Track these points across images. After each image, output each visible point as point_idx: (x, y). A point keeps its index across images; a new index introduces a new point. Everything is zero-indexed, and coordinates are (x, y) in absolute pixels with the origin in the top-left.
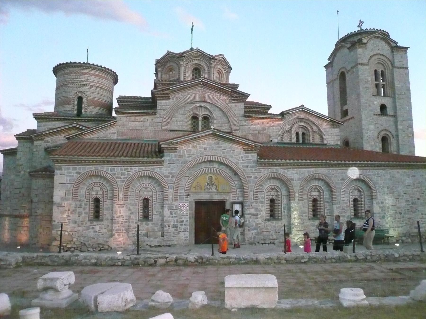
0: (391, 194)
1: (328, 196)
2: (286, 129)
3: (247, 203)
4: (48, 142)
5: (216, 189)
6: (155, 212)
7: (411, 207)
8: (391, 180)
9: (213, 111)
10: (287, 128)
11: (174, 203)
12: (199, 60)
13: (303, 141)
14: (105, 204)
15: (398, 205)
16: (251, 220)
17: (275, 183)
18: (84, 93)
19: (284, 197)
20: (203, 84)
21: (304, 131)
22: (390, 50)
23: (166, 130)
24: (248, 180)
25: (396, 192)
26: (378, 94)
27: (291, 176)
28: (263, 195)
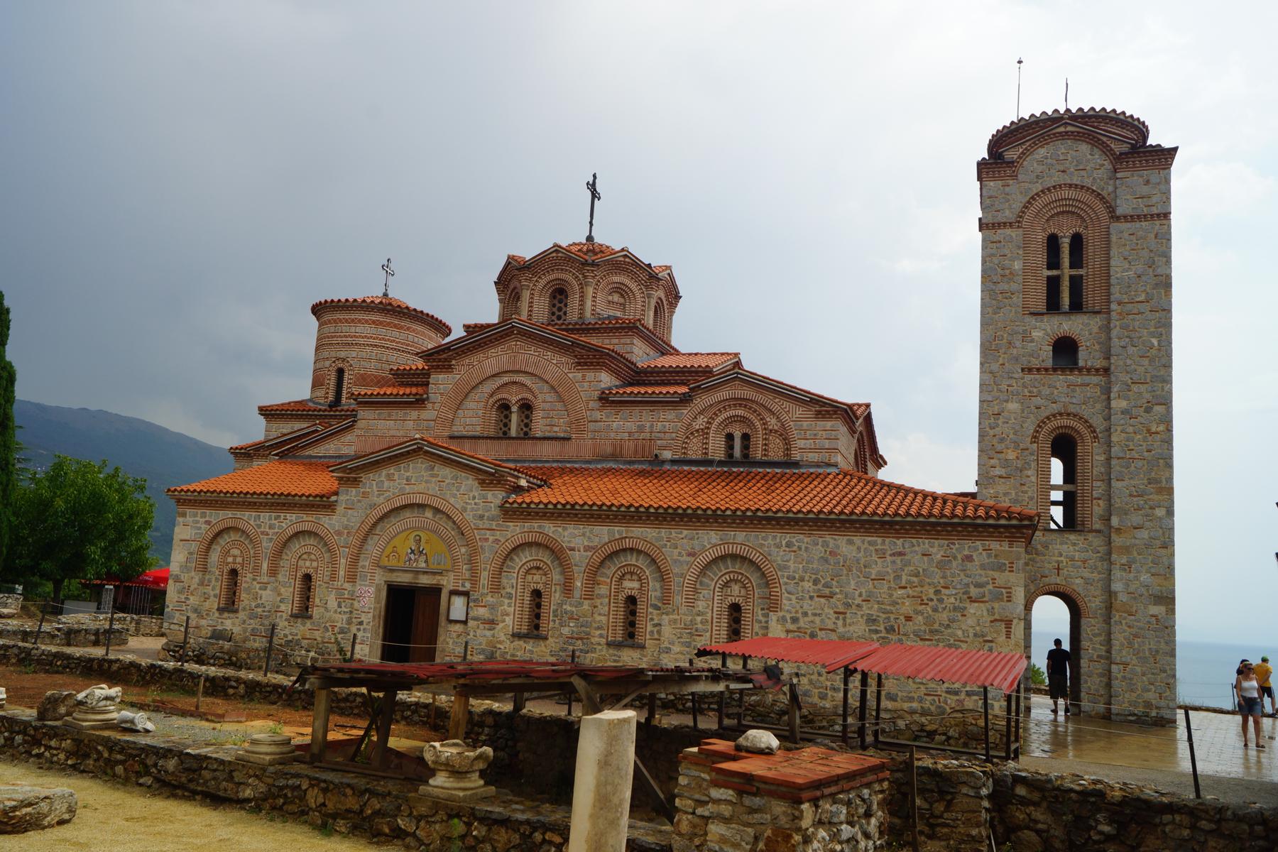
0: (823, 600)
1: (658, 594)
2: (697, 427)
3: (473, 595)
5: (426, 562)
6: (317, 601)
7: (883, 638)
8: (826, 561)
9: (537, 392)
10: (700, 422)
11: (347, 586)
12: (562, 270)
13: (746, 456)
14: (245, 580)
15: (841, 630)
16: (479, 632)
17: (540, 555)
18: (348, 362)
19: (558, 587)
21: (748, 431)
22: (1108, 165)
24: (481, 546)
25: (838, 596)
26: (1053, 305)
27: (569, 542)
28: (514, 581)
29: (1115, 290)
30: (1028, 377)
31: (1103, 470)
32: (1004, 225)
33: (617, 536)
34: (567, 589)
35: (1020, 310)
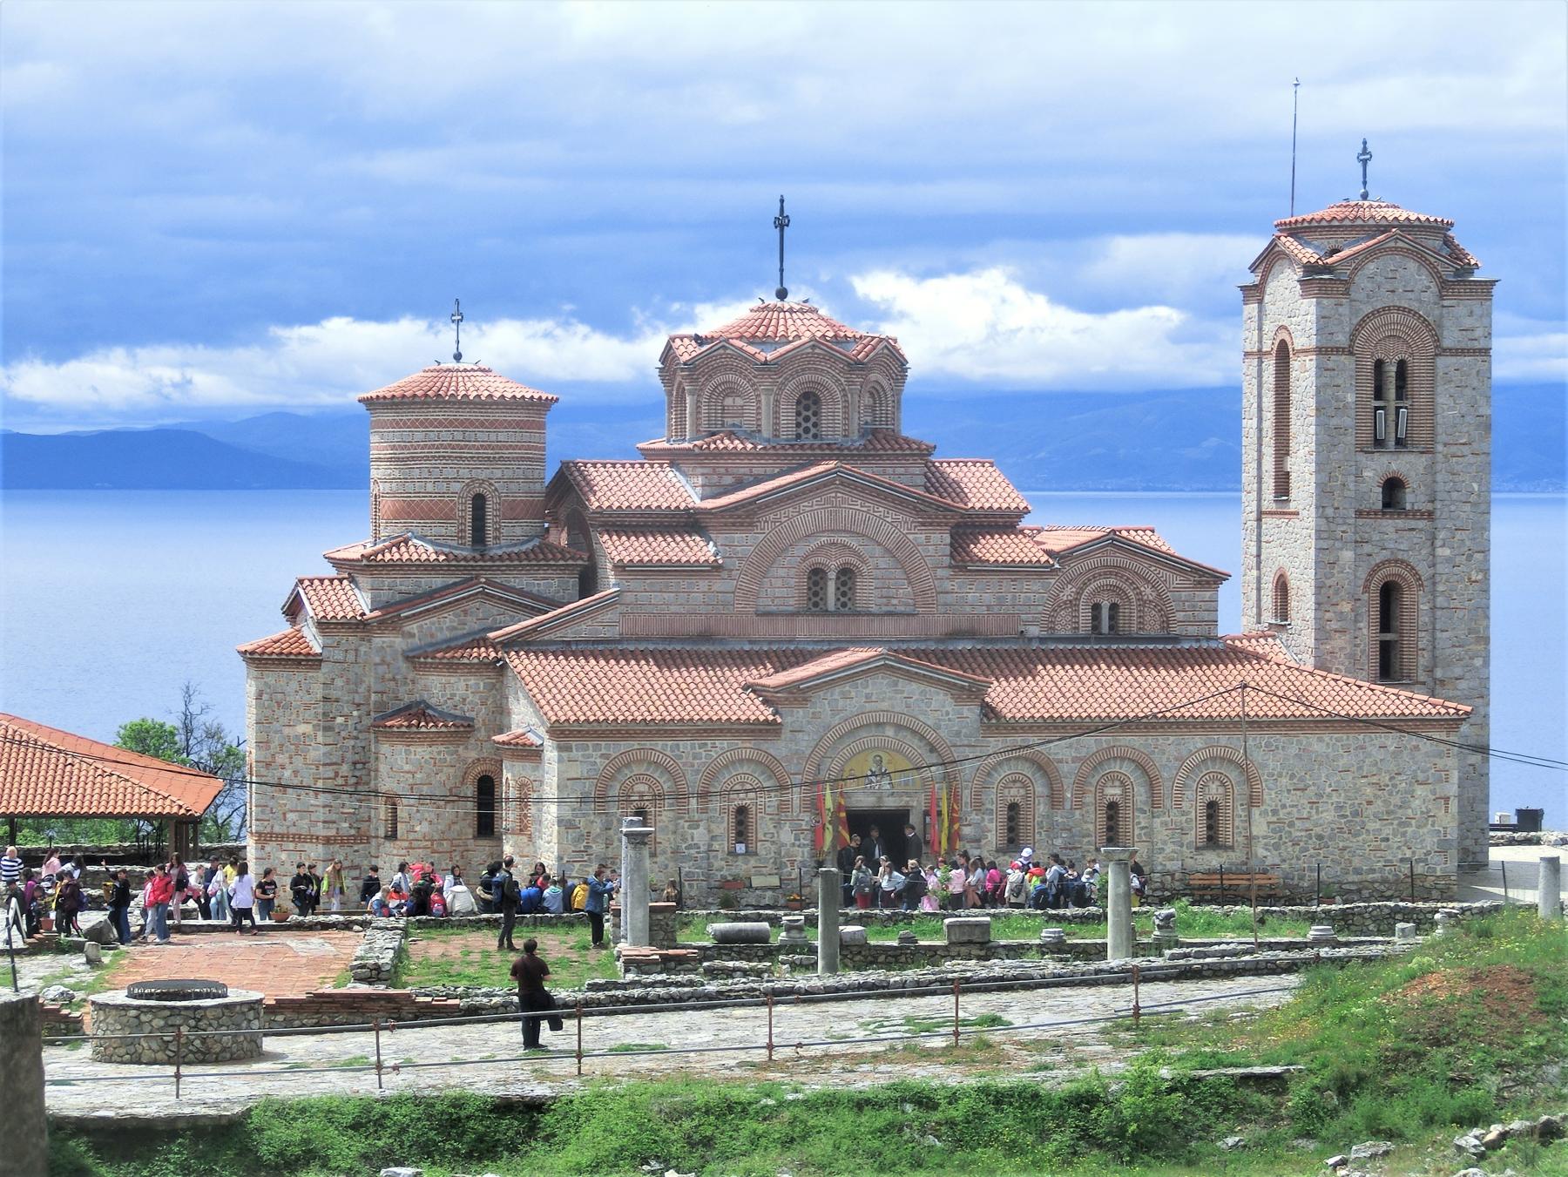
1: (1143, 798)
4: (413, 636)
6: (761, 836)
7: (1350, 821)
10: (1068, 593)
13: (1111, 628)
20: (842, 484)
21: (1116, 600)
22: (1434, 289)
23: (747, 613)
29: (1440, 430)
30: (1360, 522)
31: (1427, 619)
32: (1337, 350)
33: (1105, 746)
34: (1055, 800)
35: (1353, 448)
